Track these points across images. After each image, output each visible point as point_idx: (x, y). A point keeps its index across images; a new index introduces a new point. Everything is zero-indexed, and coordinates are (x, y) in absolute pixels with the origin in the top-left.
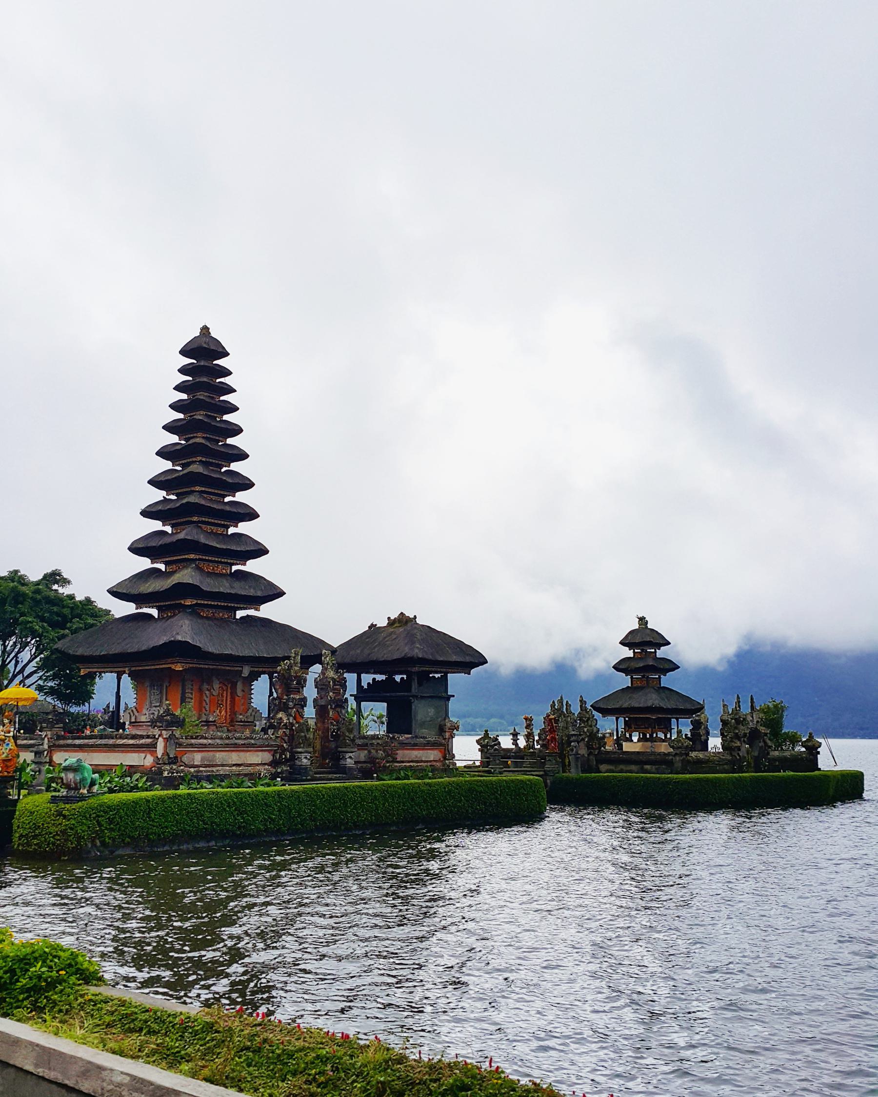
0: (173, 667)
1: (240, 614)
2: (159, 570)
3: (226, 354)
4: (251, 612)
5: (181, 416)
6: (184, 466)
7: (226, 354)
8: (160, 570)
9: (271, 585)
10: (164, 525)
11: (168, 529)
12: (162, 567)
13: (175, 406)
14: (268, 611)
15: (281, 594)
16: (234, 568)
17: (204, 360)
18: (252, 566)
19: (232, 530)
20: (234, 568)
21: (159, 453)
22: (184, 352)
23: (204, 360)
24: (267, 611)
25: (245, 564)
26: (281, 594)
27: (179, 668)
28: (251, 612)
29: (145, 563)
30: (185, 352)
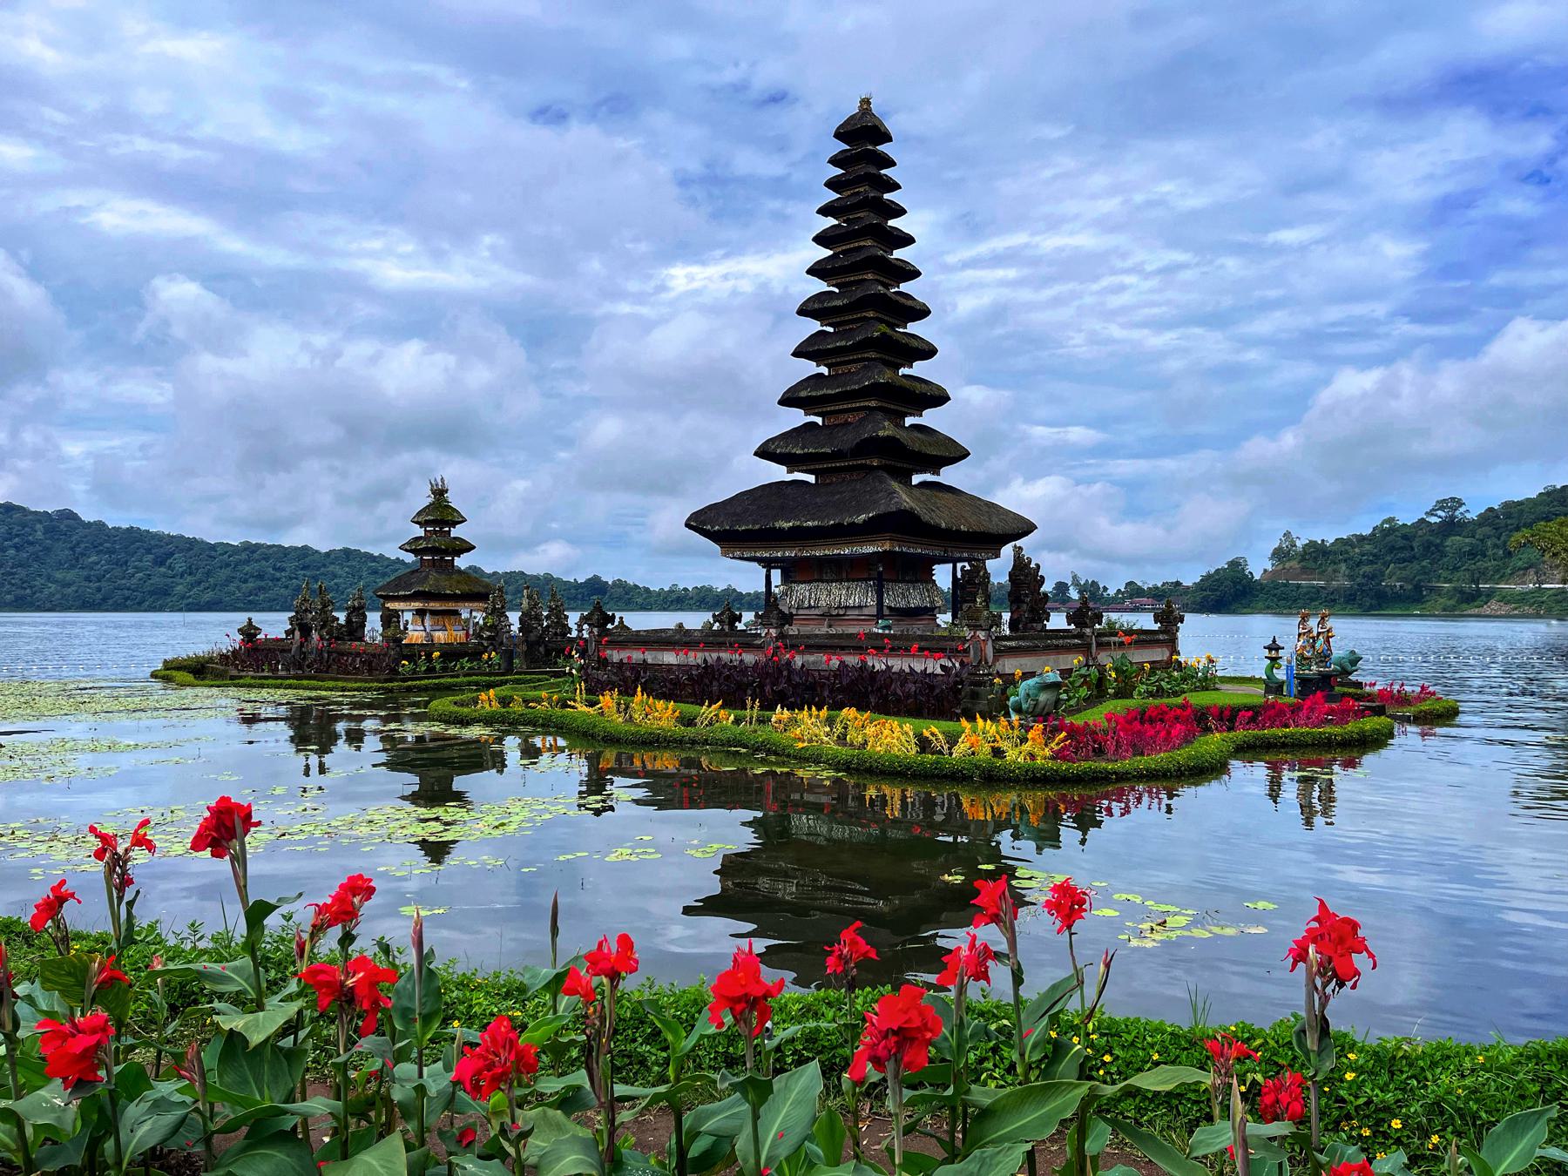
3: (887, 138)
4: (928, 477)
7: (887, 138)
11: (824, 370)
12: (819, 420)
14: (949, 476)
17: (863, 146)
18: (930, 418)
19: (903, 371)
20: (909, 421)
21: (811, 271)
22: (839, 135)
23: (863, 146)
28: (928, 477)
29: (797, 418)
30: (839, 135)
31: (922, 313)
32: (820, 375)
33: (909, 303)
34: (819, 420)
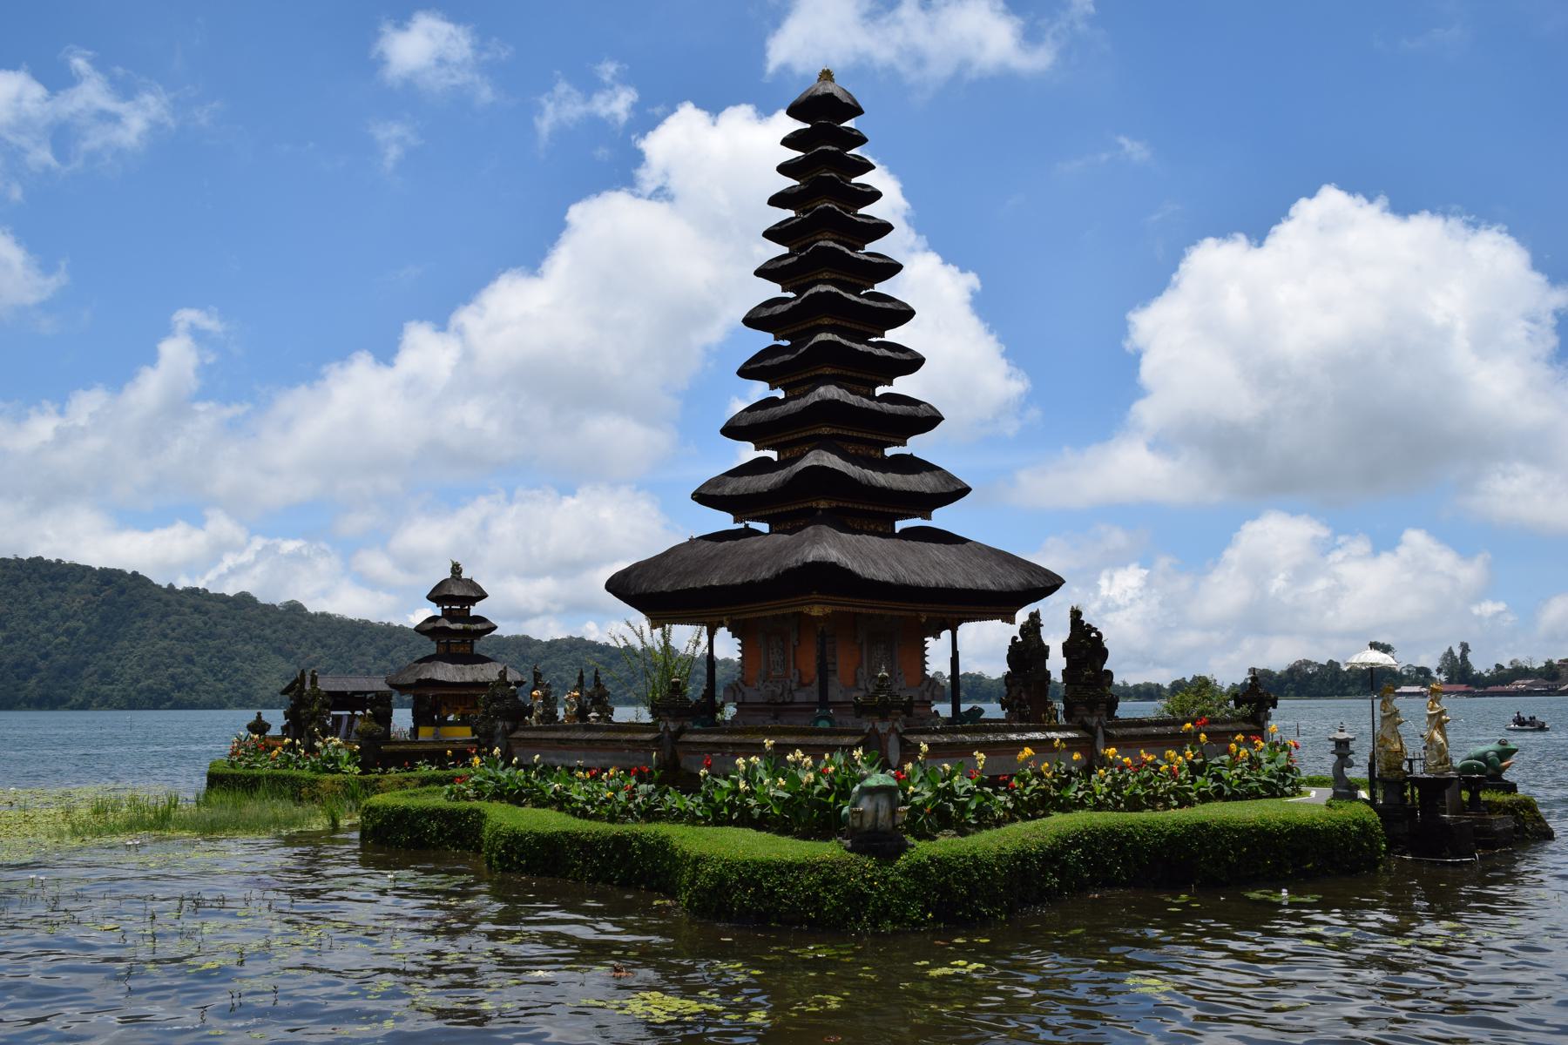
0: (806, 610)
1: (900, 525)
2: (769, 459)
5: (791, 213)
6: (800, 291)
8: (770, 459)
9: (950, 478)
10: (772, 388)
12: (773, 455)
13: (784, 169)
14: (942, 518)
15: (967, 490)
16: (889, 452)
24: (942, 518)
25: (904, 444)
26: (967, 490)
27: (816, 611)
29: (747, 452)
31: (903, 314)
32: (772, 402)
33: (888, 305)
34: (773, 455)
